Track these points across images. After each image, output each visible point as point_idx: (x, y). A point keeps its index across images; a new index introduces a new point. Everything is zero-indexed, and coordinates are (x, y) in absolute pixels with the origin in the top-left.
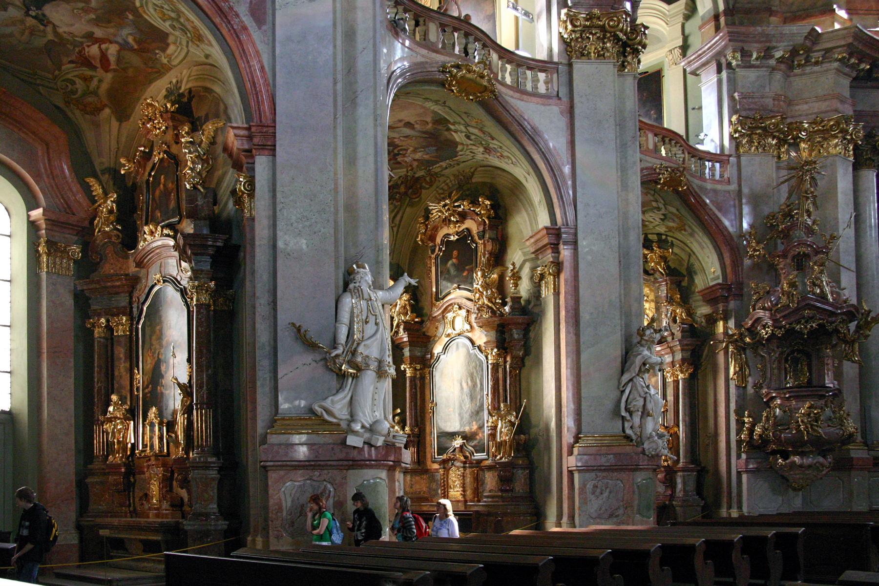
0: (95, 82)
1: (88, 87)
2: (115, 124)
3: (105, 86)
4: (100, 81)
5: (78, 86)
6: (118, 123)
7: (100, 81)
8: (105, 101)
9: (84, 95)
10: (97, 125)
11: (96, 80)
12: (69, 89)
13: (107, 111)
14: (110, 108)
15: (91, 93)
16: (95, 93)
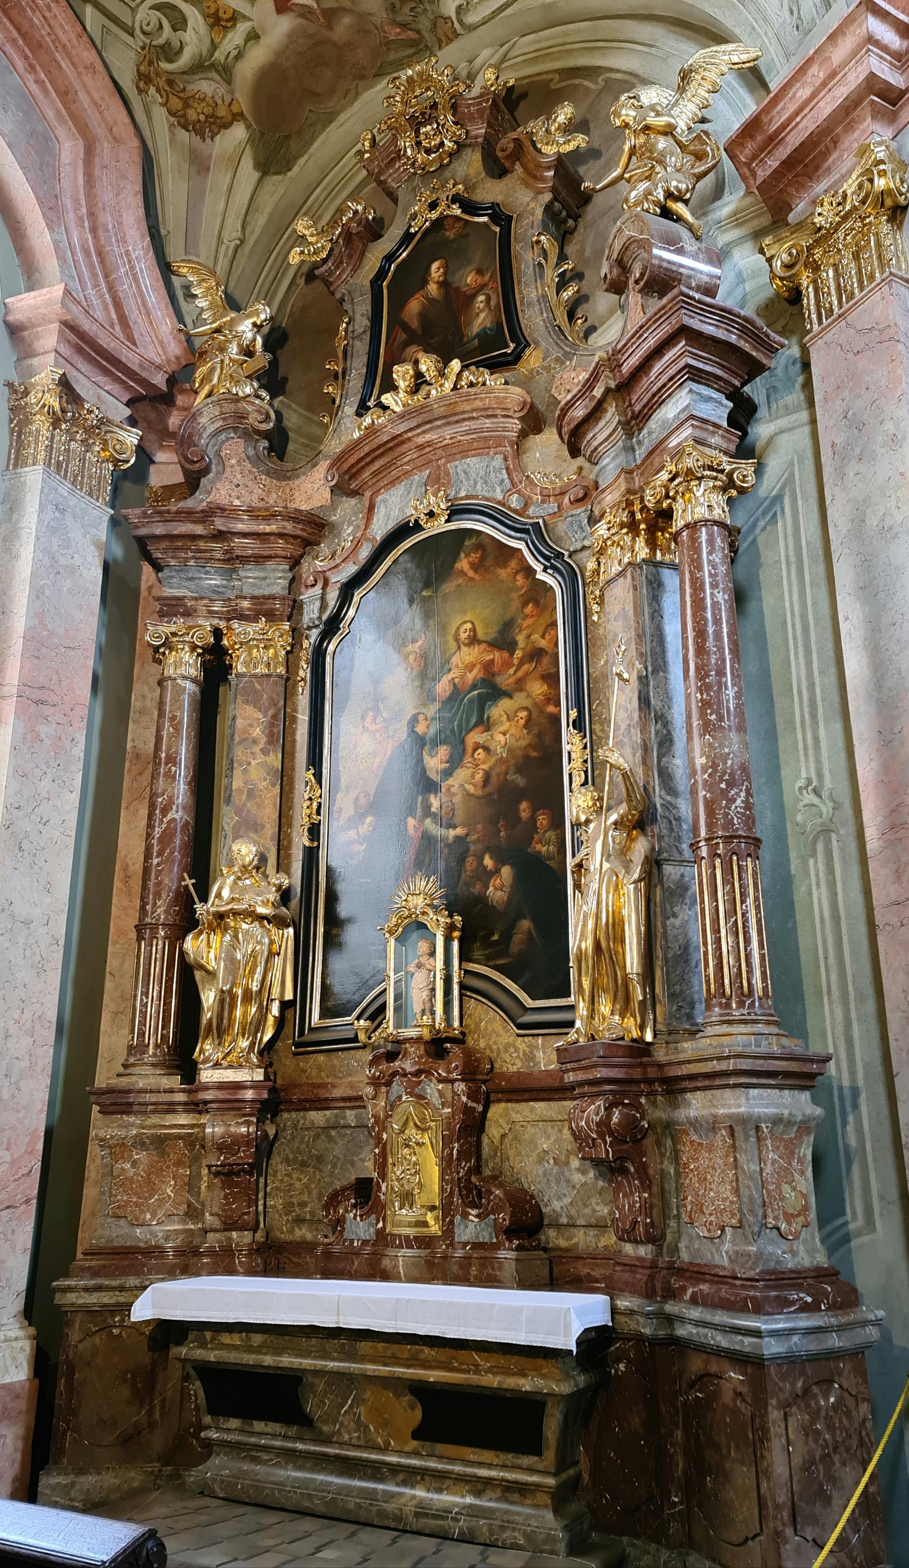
0: (235, 38)
1: (214, 46)
2: (248, 173)
3: (258, 57)
4: (253, 36)
5: (189, 36)
6: (256, 175)
7: (253, 36)
8: (243, 102)
9: (199, 67)
10: (200, 165)
11: (242, 28)
12: (161, 41)
13: (239, 133)
14: (248, 127)
15: (213, 66)
16: (226, 72)
